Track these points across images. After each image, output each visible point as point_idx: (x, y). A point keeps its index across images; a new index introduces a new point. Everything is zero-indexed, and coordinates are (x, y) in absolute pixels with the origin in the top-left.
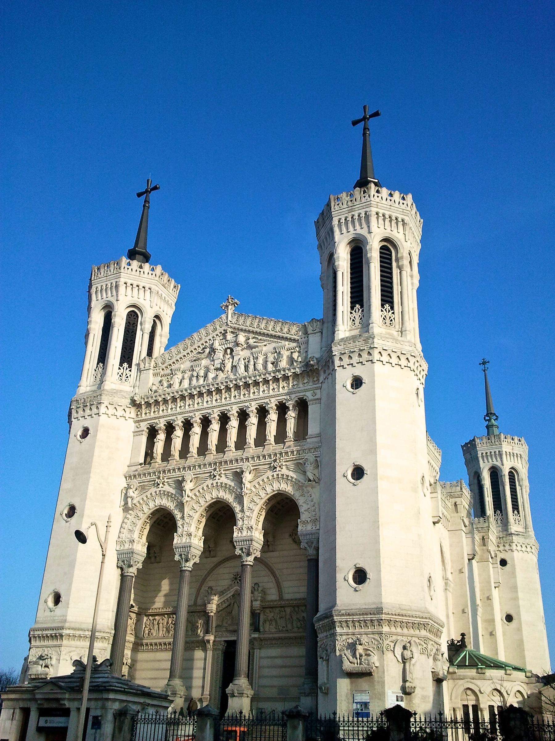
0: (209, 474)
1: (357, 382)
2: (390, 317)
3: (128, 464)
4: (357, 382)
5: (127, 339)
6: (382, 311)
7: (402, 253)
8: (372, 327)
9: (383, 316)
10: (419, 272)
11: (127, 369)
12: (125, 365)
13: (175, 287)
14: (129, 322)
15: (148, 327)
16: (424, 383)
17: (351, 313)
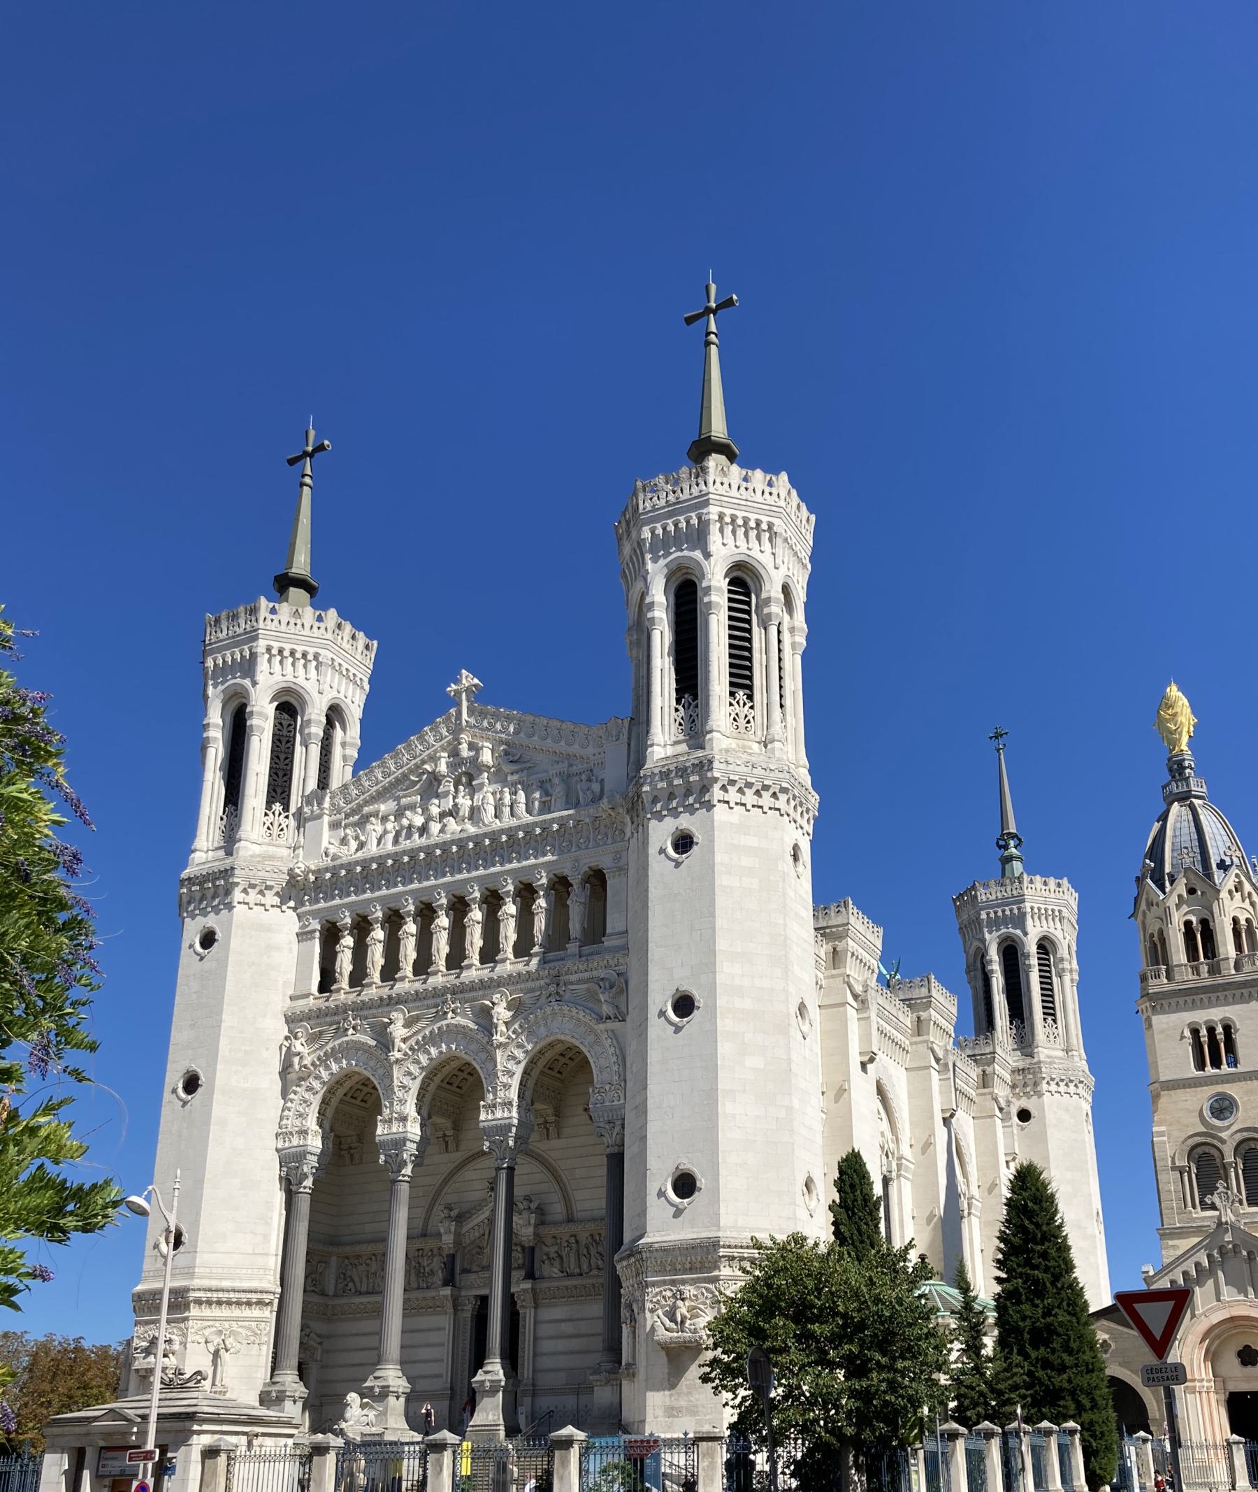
0: (434, 1010)
1: (684, 843)
2: (746, 716)
3: (291, 992)
4: (684, 843)
5: (278, 757)
6: (731, 704)
7: (769, 591)
8: (711, 740)
9: (733, 715)
10: (808, 620)
11: (280, 814)
12: (277, 807)
13: (367, 647)
14: (281, 724)
15: (317, 731)
16: (811, 832)
17: (677, 710)
